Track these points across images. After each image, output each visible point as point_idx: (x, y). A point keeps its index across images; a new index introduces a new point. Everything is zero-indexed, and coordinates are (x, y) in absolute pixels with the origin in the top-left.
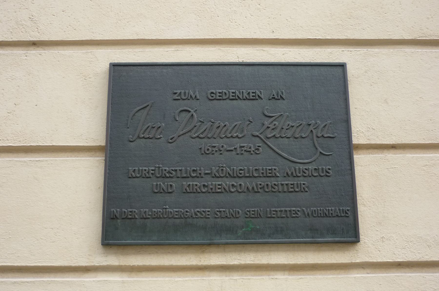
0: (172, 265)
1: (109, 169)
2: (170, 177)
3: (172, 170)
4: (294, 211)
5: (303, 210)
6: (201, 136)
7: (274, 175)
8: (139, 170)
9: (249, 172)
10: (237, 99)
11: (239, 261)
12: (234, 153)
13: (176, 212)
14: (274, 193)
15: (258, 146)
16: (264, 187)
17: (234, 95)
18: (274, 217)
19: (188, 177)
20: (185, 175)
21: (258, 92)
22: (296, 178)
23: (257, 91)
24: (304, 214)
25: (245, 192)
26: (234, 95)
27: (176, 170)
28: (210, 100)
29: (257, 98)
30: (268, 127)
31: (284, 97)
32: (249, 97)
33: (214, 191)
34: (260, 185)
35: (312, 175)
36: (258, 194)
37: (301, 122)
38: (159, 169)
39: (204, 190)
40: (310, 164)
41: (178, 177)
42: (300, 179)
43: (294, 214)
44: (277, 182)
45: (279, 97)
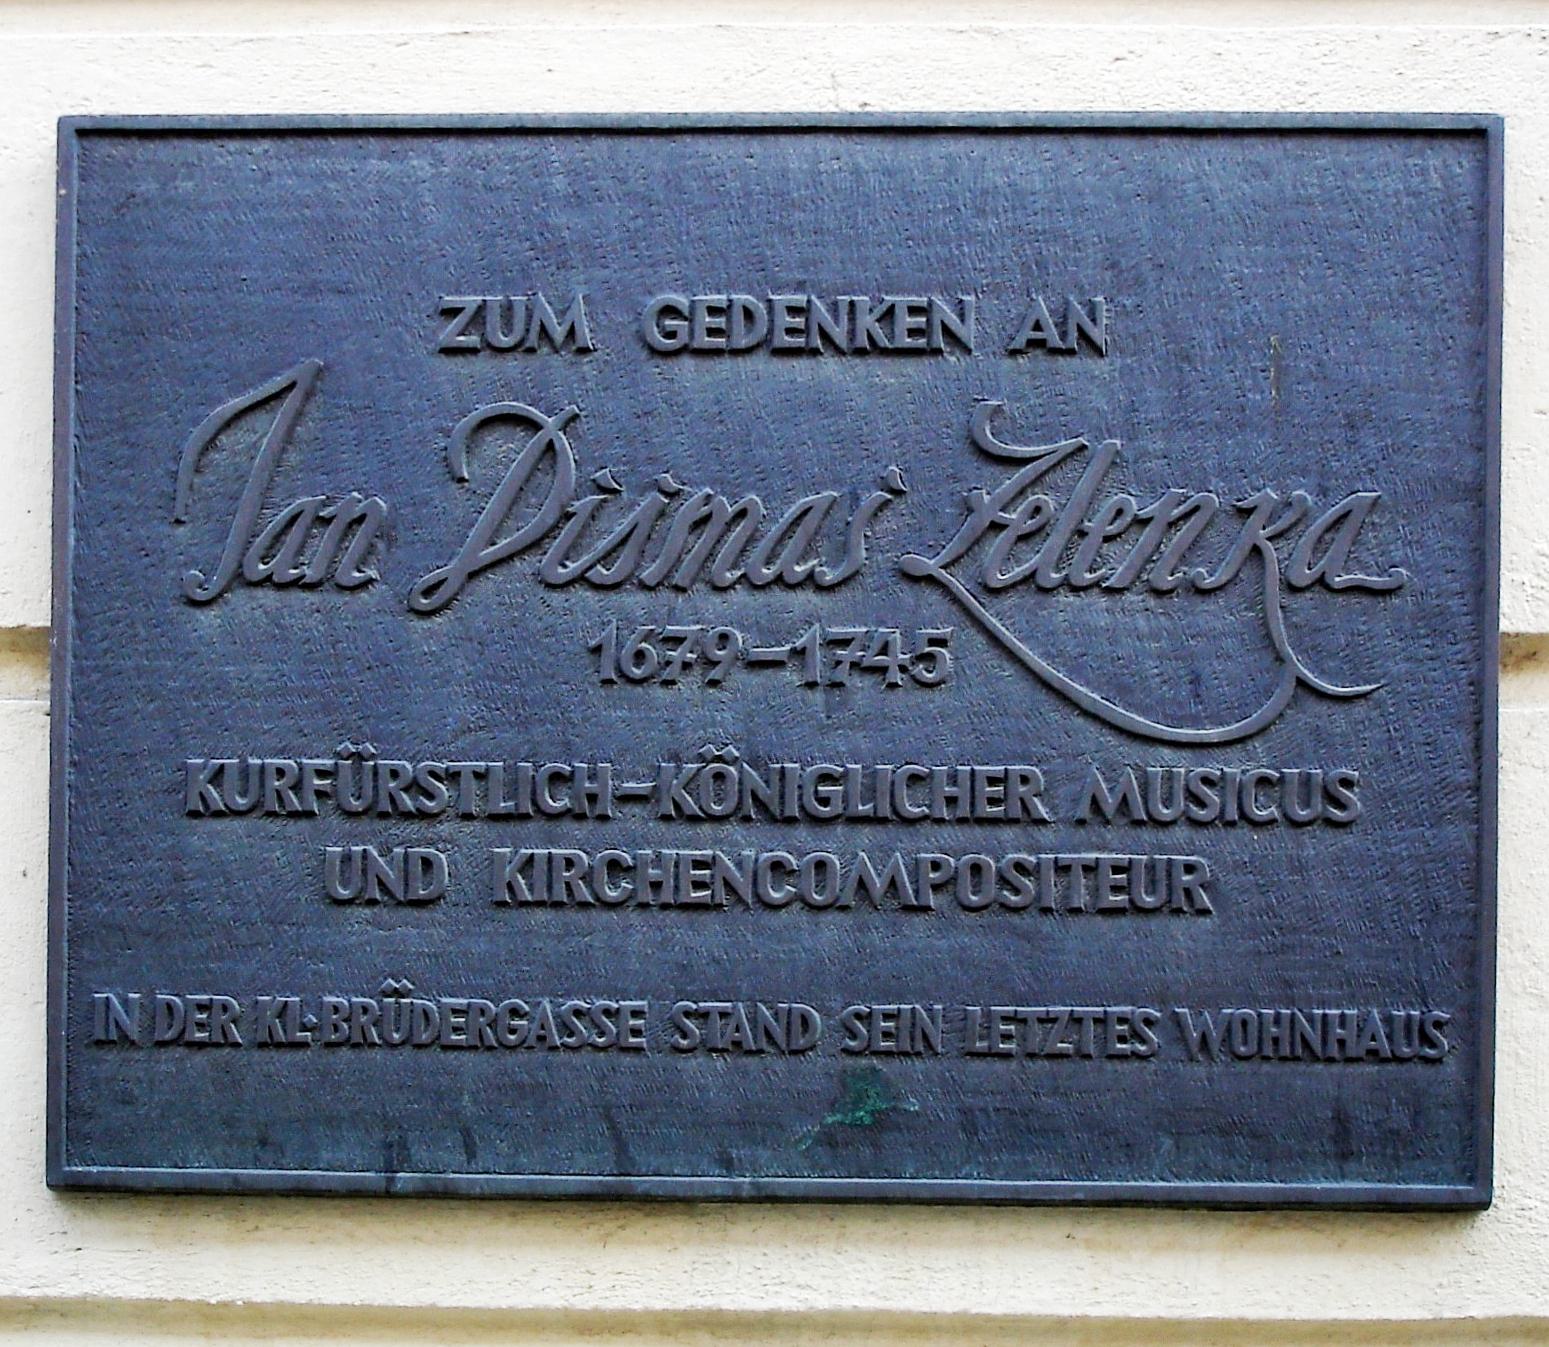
0: (433, 1308)
1: (74, 764)
2: (422, 815)
3: (433, 774)
4: (1122, 1020)
5: (1177, 1020)
6: (601, 573)
7: (1016, 812)
8: (245, 771)
9: (870, 793)
10: (814, 352)
11: (805, 1294)
12: (790, 676)
13: (456, 1012)
14: (1015, 919)
15: (933, 642)
16: (953, 880)
17: (798, 321)
18: (1006, 1056)
19: (526, 817)
20: (504, 806)
21: (946, 311)
22: (1147, 835)
23: (938, 300)
24: (1182, 1038)
25: (844, 908)
26: (798, 321)
27: (453, 777)
28: (655, 352)
29: (939, 341)
30: (997, 527)
31: (1098, 334)
32: (891, 337)
33: (667, 896)
34: (936, 866)
35: (1243, 815)
36: (918, 920)
37: (1197, 497)
38: (358, 770)
39: (612, 894)
40: (1234, 752)
41: (468, 817)
42: (1163, 836)
43: (1122, 1039)
44: (1036, 850)
45: (1073, 340)
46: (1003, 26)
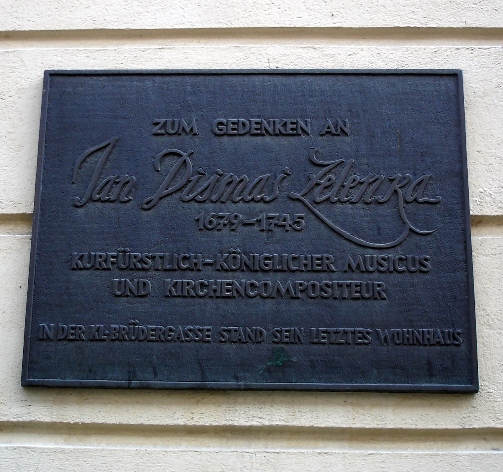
0: (142, 424)
1: (38, 254)
2: (144, 269)
3: (147, 257)
4: (360, 332)
7: (325, 268)
8: (90, 256)
9: (281, 263)
10: (263, 135)
11: (261, 420)
12: (256, 228)
13: (152, 330)
14: (326, 301)
15: (299, 218)
17: (259, 126)
18: (324, 344)
19: (175, 270)
21: (301, 123)
22: (366, 275)
23: (299, 120)
25: (273, 298)
26: (259, 126)
27: (153, 258)
28: (216, 135)
29: (300, 132)
30: (318, 184)
31: (346, 130)
32: (286, 131)
33: (218, 294)
34: (301, 285)
35: (395, 269)
36: (296, 301)
37: (377, 176)
38: (124, 256)
39: (201, 293)
41: (157, 270)
42: (371, 276)
43: (360, 338)
45: (339, 131)
46: (317, 46)
